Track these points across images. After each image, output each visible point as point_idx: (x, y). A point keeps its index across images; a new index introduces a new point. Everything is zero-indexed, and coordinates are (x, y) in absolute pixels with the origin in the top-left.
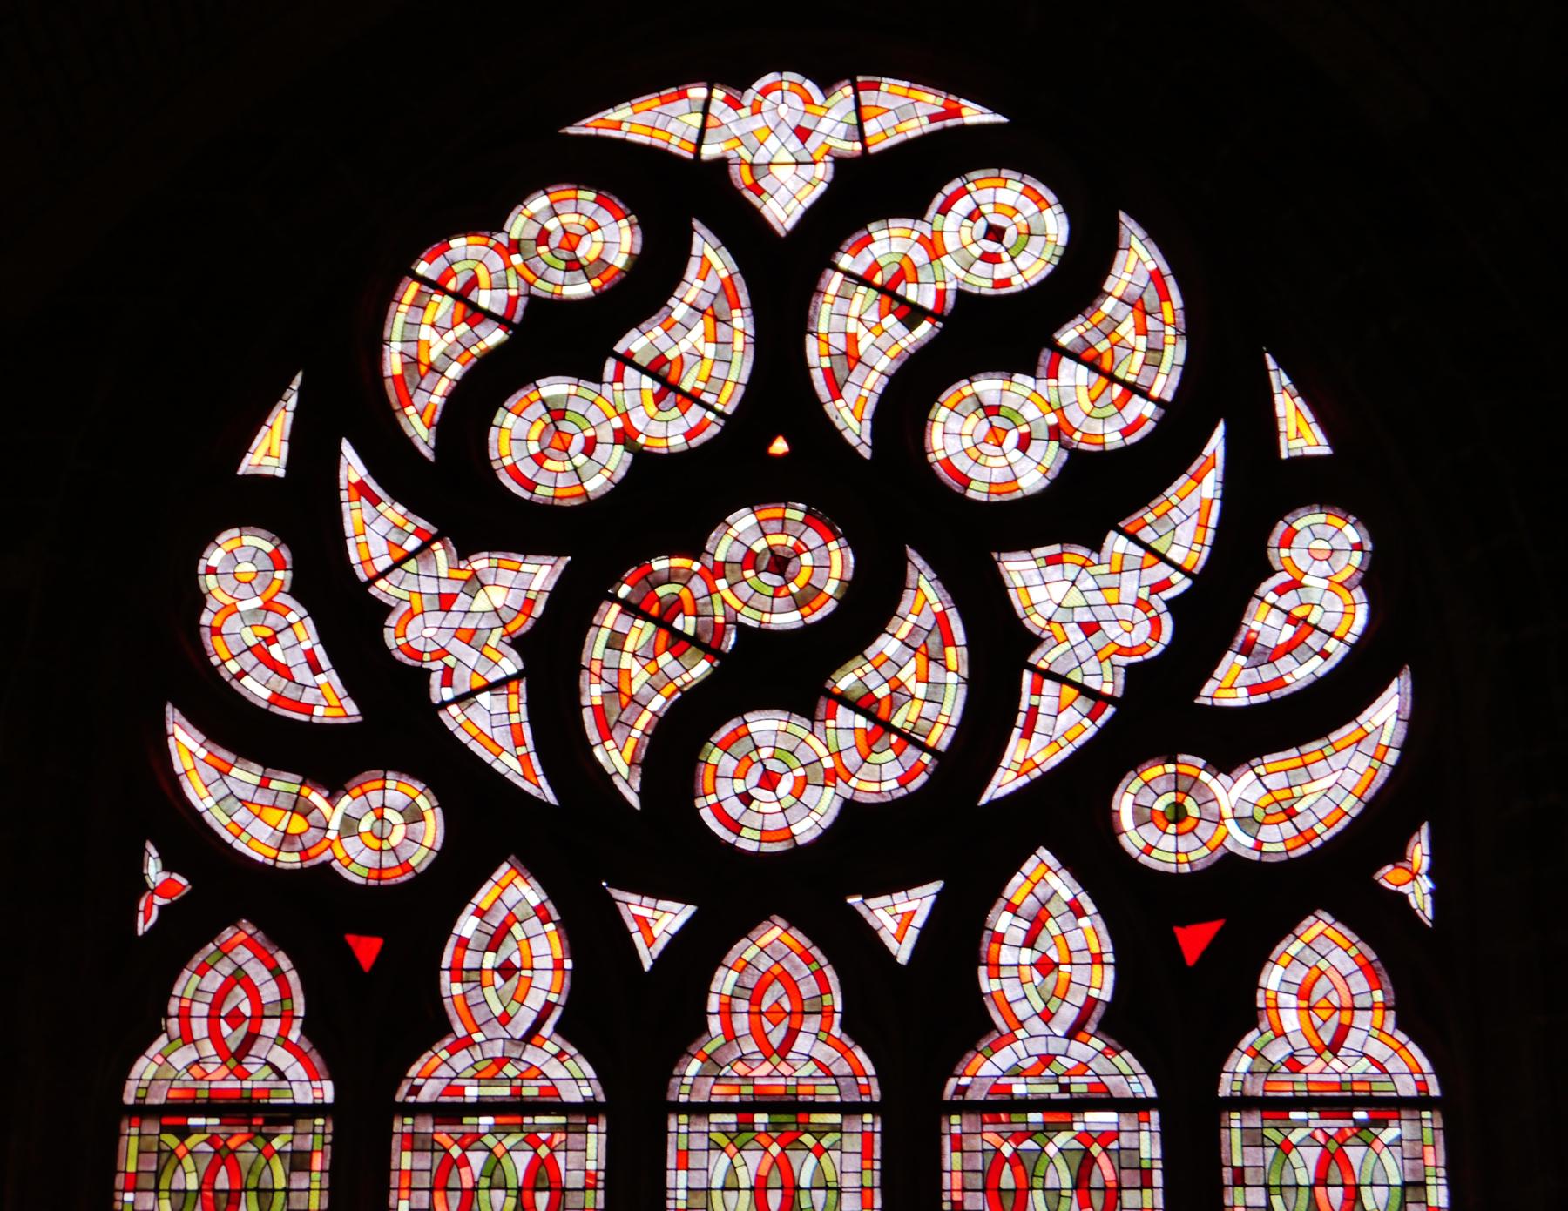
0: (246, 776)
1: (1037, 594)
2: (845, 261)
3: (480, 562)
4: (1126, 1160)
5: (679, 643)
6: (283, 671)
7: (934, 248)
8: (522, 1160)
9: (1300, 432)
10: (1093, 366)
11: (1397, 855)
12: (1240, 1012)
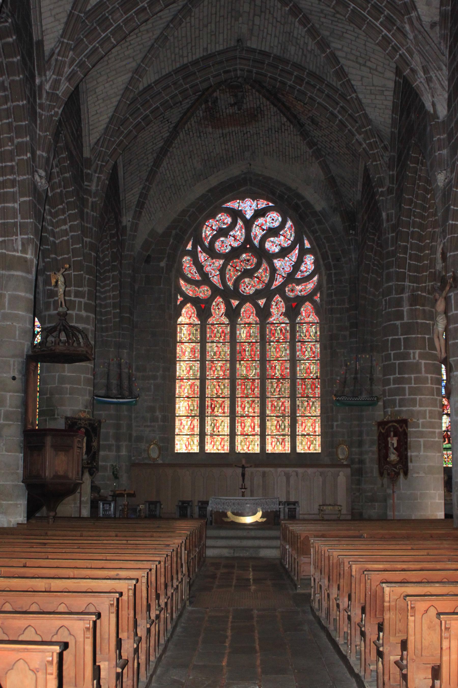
0: (189, 286)
1: (277, 264)
2: (256, 223)
3: (214, 260)
4: (286, 330)
5: (237, 271)
6: (192, 274)
7: (266, 221)
8: (221, 330)
9: (307, 245)
10: (284, 236)
11: (316, 295)
12: (298, 313)
